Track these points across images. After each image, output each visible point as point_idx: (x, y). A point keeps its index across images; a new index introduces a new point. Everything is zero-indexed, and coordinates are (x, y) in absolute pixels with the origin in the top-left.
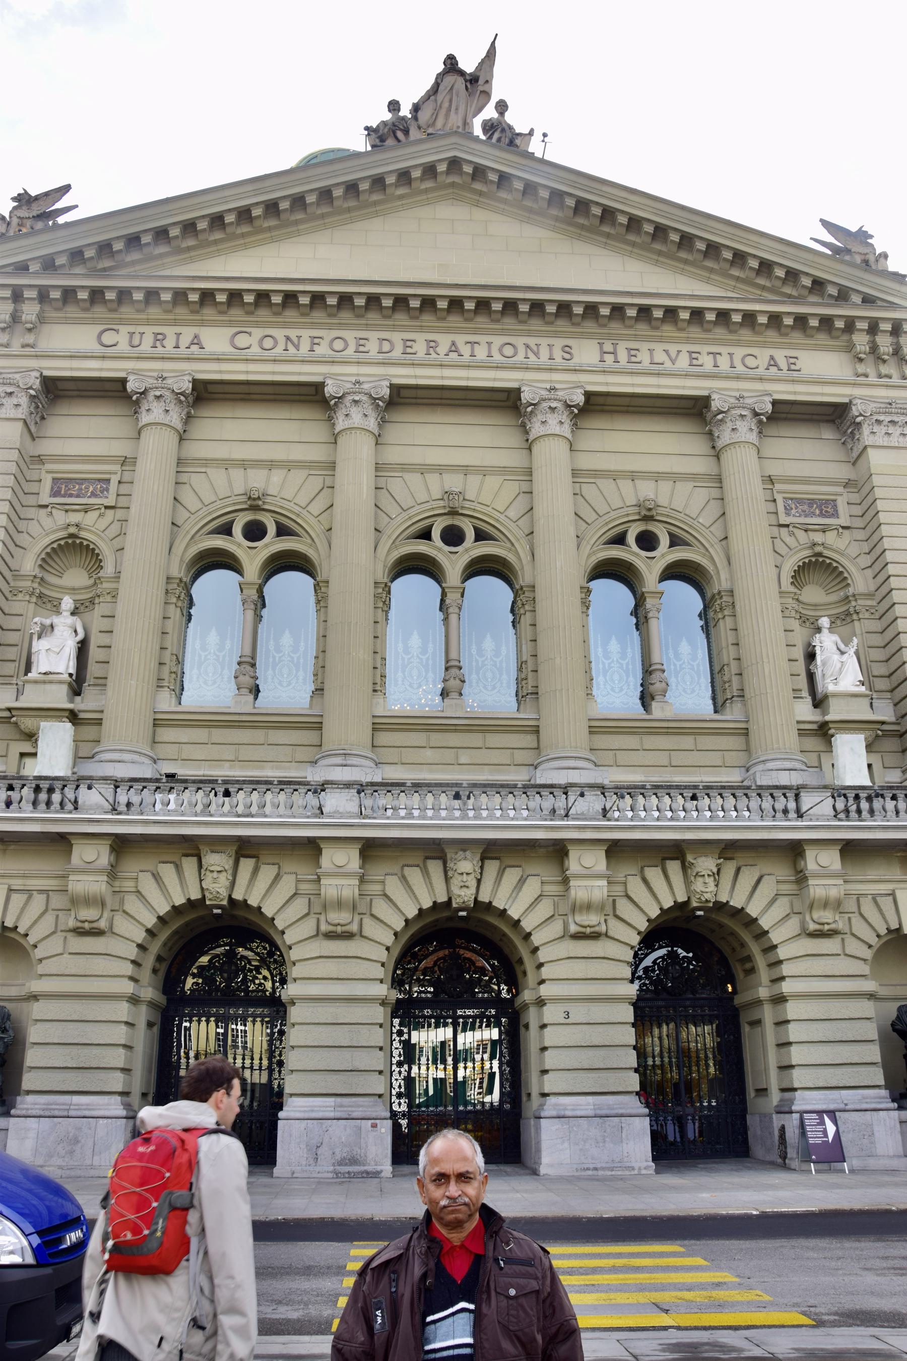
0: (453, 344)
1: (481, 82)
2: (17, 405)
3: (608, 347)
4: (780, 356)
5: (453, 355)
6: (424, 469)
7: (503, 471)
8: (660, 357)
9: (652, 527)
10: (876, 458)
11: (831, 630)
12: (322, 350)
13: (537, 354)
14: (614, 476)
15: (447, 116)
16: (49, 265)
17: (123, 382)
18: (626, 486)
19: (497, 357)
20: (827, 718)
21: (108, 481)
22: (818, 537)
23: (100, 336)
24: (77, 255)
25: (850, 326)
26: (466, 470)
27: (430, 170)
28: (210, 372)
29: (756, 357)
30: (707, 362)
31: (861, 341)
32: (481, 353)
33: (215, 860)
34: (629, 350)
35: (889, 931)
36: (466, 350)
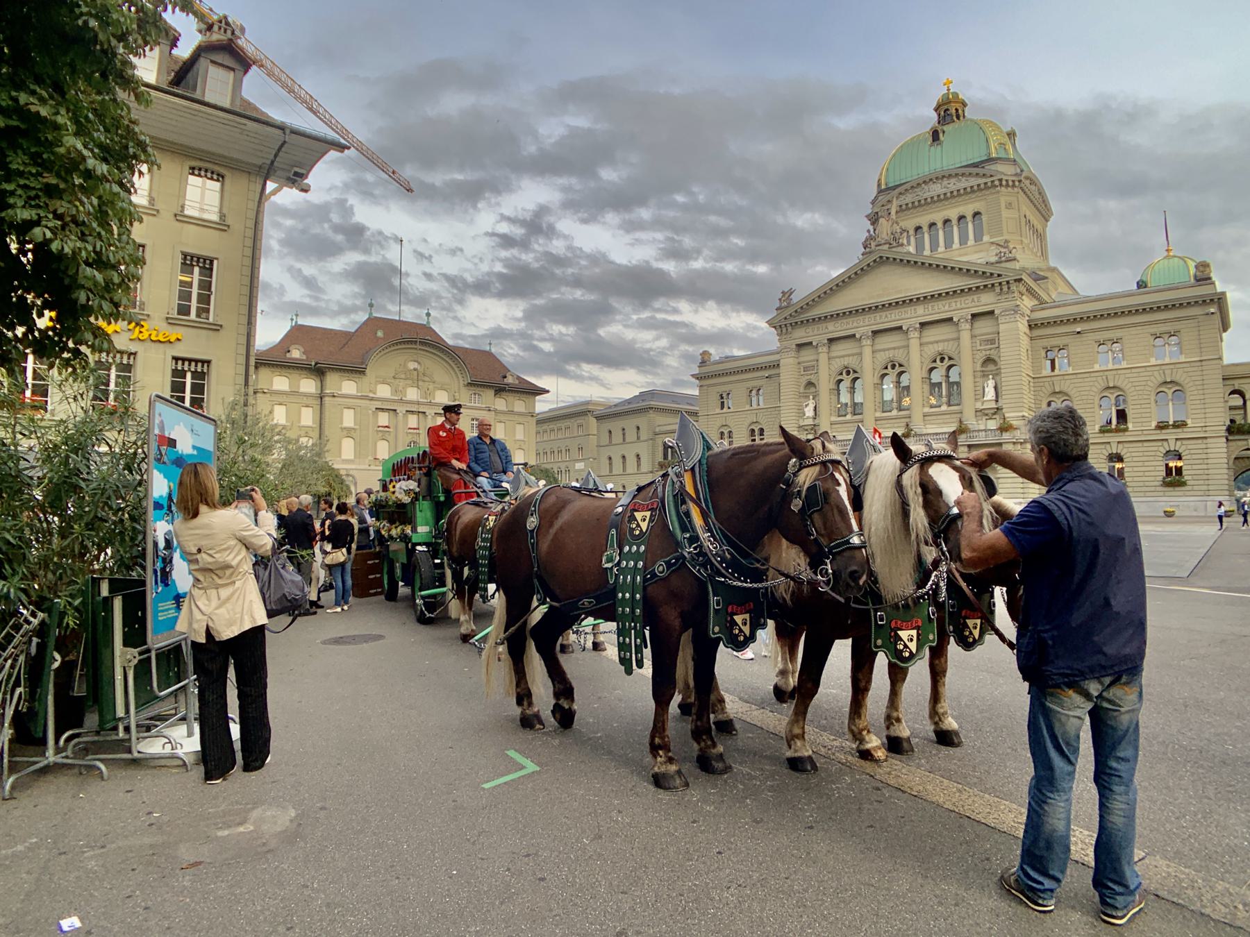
4: (975, 297)
6: (884, 350)
7: (904, 347)
8: (941, 306)
10: (1002, 327)
12: (855, 324)
14: (932, 343)
16: (791, 315)
17: (811, 343)
18: (935, 345)
22: (988, 353)
25: (993, 285)
26: (894, 348)
27: (875, 261)
30: (954, 304)
31: (998, 289)
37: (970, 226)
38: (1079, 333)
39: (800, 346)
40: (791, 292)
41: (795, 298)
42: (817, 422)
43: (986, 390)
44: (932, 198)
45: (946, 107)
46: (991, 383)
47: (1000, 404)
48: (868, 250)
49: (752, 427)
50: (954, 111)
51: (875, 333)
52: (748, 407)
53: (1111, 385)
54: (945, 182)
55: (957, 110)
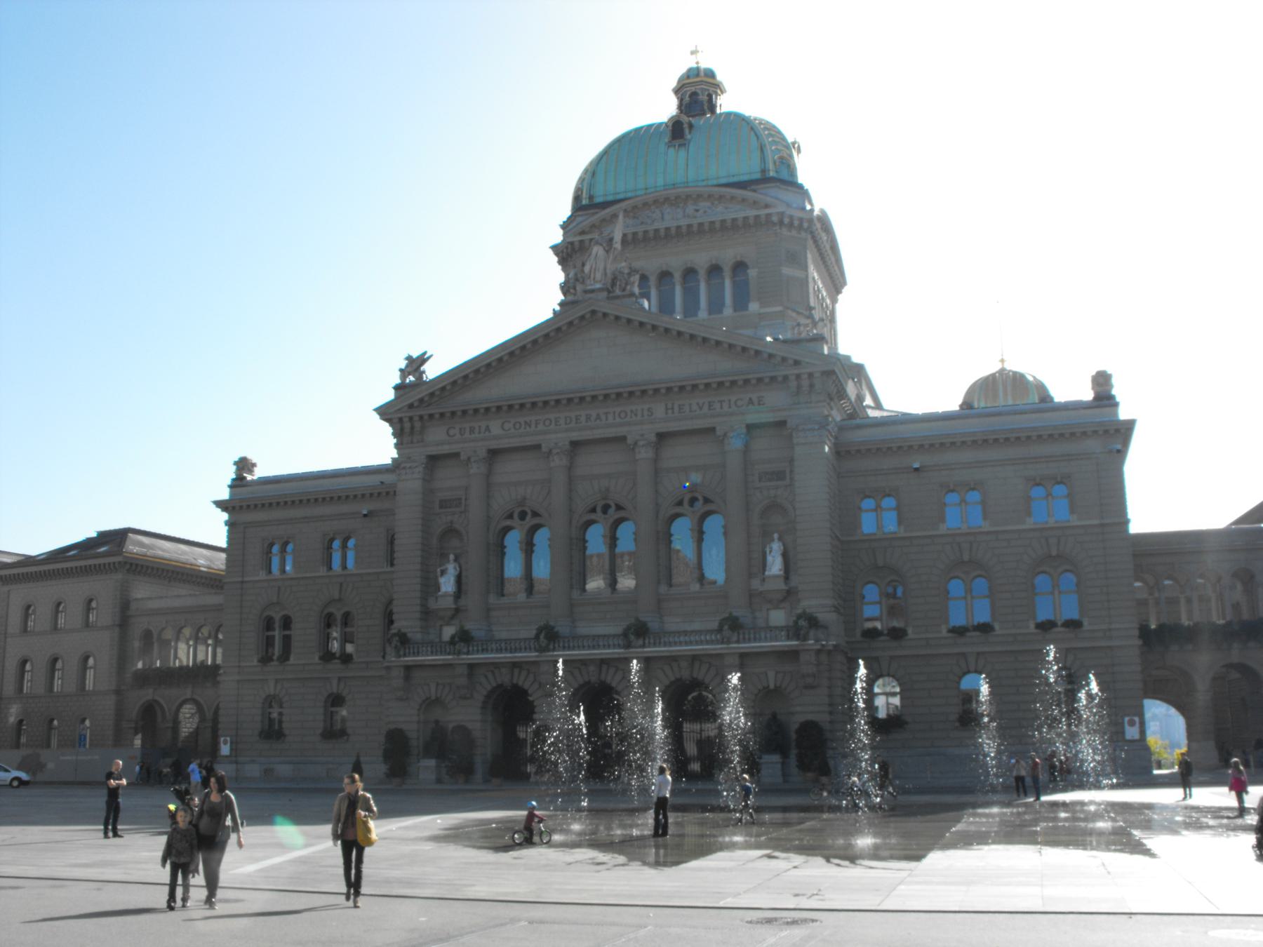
0: (598, 415)
1: (614, 241)
2: (419, 472)
3: (670, 406)
4: (754, 397)
5: (598, 421)
8: (695, 407)
9: (697, 495)
11: (780, 539)
12: (541, 427)
13: (636, 415)
15: (595, 273)
16: (421, 401)
19: (618, 420)
20: (761, 590)
21: (460, 499)
23: (447, 433)
24: (432, 395)
25: (786, 378)
27: (582, 318)
28: (494, 445)
29: (741, 400)
30: (717, 406)
31: (793, 384)
32: (610, 419)
33: (504, 670)
34: (680, 405)
35: (764, 688)
36: (603, 417)
37: (728, 284)
38: (916, 470)
39: (433, 460)
40: (423, 359)
41: (432, 371)
42: (462, 602)
43: (769, 559)
44: (667, 229)
45: (693, 89)
46: (776, 547)
47: (795, 581)
48: (570, 298)
49: (331, 609)
50: (706, 98)
51: (575, 444)
52: (323, 571)
53: (966, 557)
54: (690, 209)
55: (710, 96)
